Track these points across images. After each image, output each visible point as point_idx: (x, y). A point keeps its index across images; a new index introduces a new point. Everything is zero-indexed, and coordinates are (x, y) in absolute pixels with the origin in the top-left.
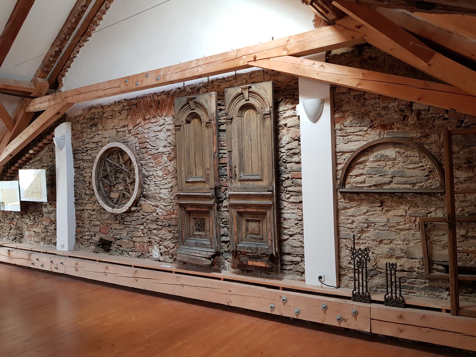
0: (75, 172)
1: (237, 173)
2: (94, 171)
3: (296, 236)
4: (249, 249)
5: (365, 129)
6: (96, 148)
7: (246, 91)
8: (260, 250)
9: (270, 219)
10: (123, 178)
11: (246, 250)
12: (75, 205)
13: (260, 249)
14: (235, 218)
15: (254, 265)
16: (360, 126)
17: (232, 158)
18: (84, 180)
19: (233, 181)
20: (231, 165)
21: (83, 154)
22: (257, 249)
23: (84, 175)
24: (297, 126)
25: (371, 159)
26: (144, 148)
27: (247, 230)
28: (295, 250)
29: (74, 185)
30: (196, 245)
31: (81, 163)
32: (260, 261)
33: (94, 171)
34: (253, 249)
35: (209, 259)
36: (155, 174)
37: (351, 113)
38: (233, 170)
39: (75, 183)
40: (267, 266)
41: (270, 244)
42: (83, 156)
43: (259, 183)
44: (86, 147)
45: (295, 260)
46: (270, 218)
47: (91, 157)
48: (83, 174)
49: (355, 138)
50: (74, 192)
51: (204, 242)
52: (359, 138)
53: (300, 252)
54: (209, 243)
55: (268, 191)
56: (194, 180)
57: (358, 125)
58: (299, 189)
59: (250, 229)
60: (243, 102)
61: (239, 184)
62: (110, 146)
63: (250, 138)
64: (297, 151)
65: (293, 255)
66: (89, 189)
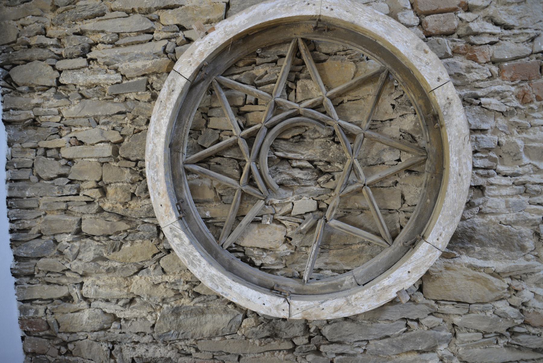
0: (10, 144)
2: (157, 133)
6: (149, 37)
10: (311, 162)
12: (14, 280)
18: (64, 176)
21: (60, 65)
23: (67, 153)
26: (447, 35)
29: (8, 198)
31: (47, 104)
33: (157, 133)
36: (520, 143)
39: (10, 189)
42: (60, 72)
44: (81, 33)
47: (117, 77)
48: (58, 149)
50: (8, 226)
62: (275, 14)
66: (101, 210)
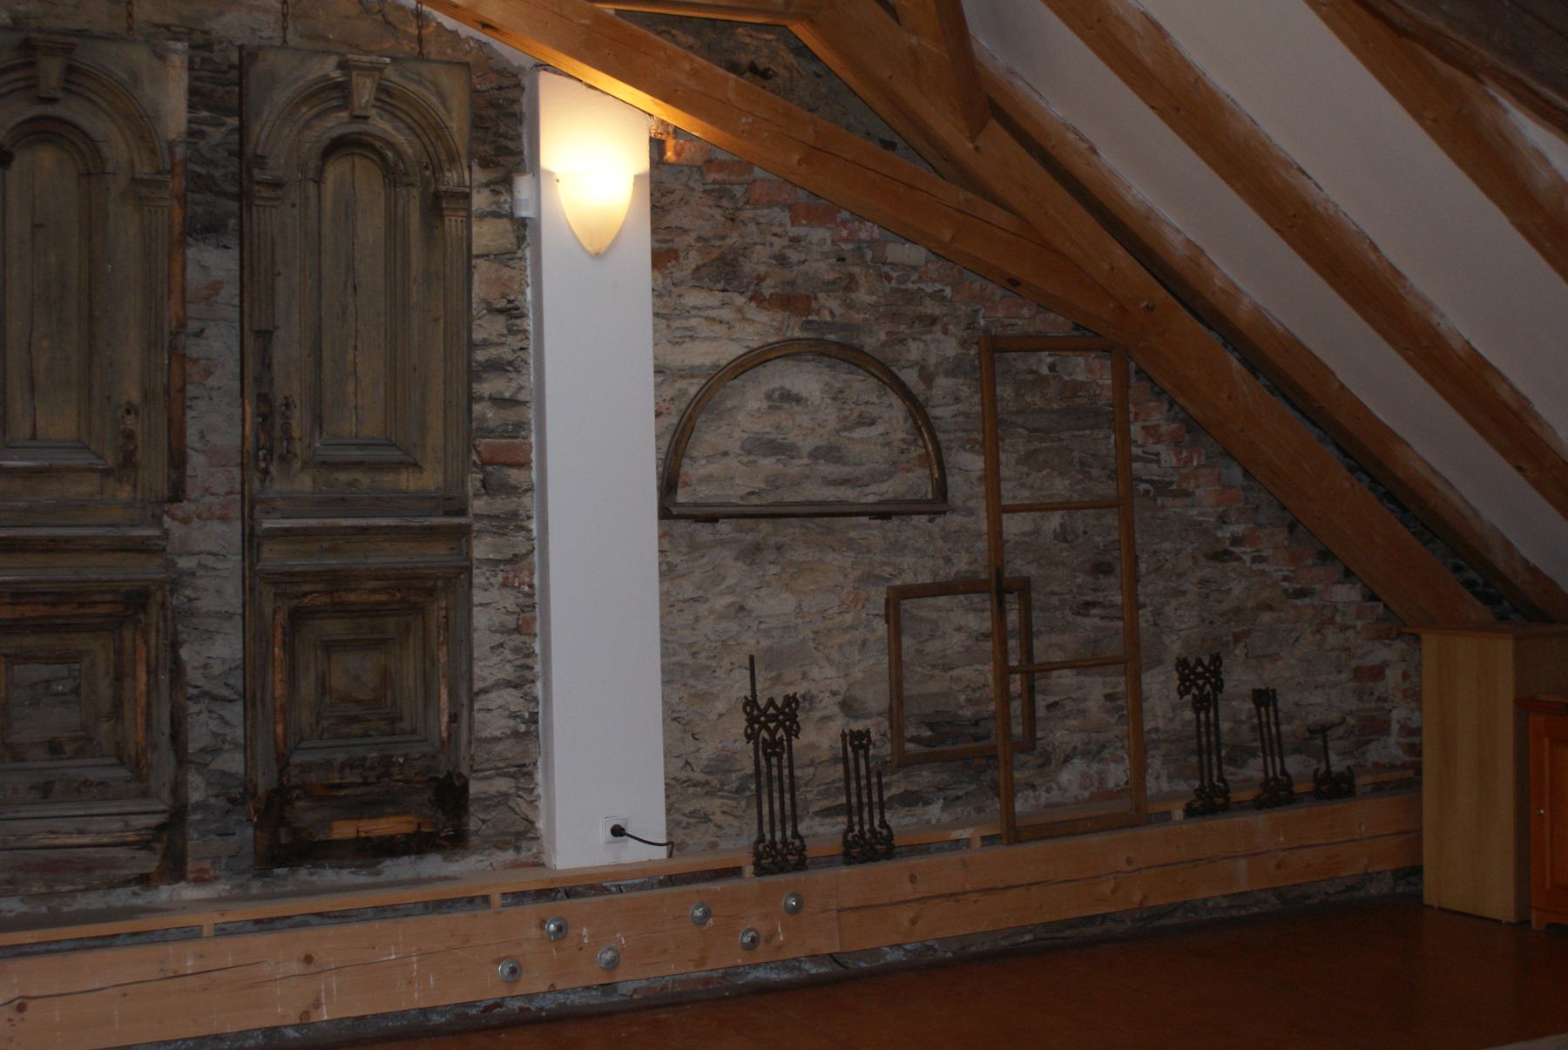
1: (296, 433)
3: (493, 695)
4: (347, 770)
5: (740, 300)
7: (369, 83)
8: (402, 765)
9: (448, 630)
11: (336, 775)
13: (401, 760)
14: (279, 636)
15: (362, 835)
16: (724, 291)
17: (275, 361)
19: (274, 469)
20: (265, 395)
22: (386, 762)
24: (507, 256)
25: (753, 405)
27: (323, 687)
28: (488, 754)
30: (45, 791)
32: (397, 814)
34: (368, 763)
35: (144, 845)
37: (699, 239)
38: (278, 421)
40: (423, 830)
41: (445, 735)
43: (408, 481)
45: (492, 790)
46: (447, 624)
49: (704, 329)
51: (94, 775)
52: (721, 330)
53: (510, 756)
54: (123, 773)
55: (447, 514)
56: (46, 464)
57: (720, 286)
58: (512, 507)
59: (338, 681)
60: (335, 124)
61: (304, 483)
63: (350, 283)
64: (506, 353)
65: (481, 774)
